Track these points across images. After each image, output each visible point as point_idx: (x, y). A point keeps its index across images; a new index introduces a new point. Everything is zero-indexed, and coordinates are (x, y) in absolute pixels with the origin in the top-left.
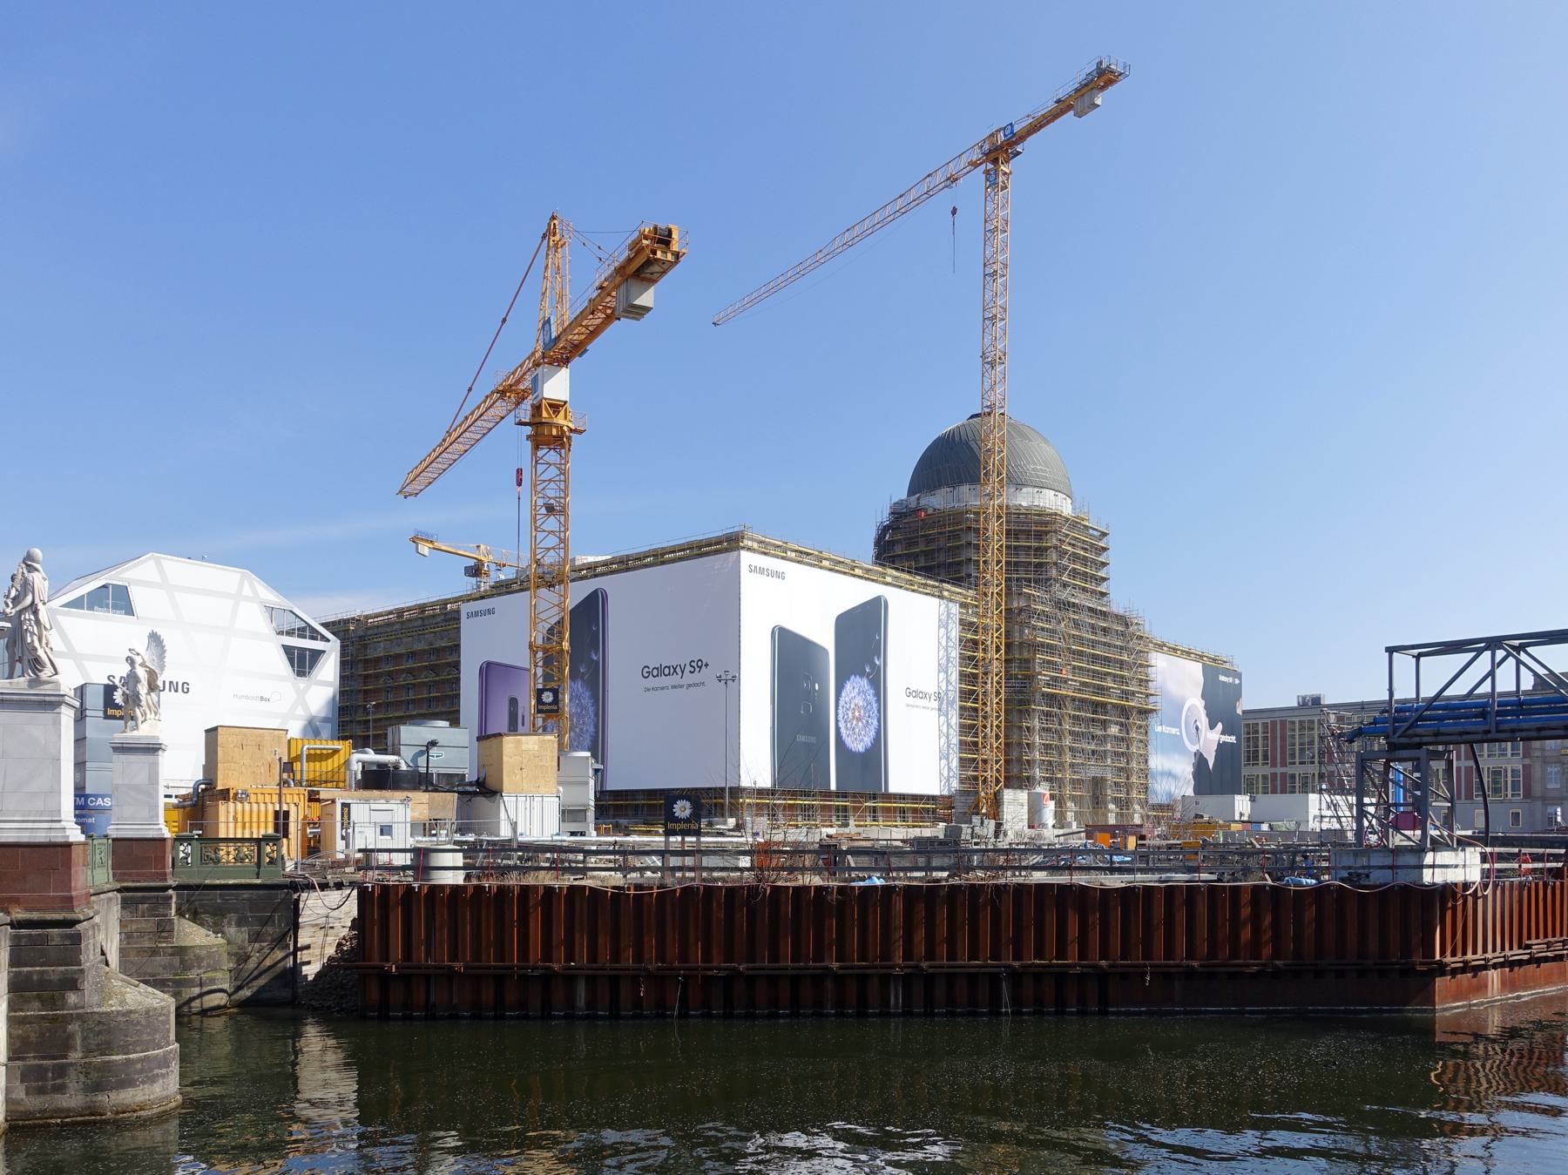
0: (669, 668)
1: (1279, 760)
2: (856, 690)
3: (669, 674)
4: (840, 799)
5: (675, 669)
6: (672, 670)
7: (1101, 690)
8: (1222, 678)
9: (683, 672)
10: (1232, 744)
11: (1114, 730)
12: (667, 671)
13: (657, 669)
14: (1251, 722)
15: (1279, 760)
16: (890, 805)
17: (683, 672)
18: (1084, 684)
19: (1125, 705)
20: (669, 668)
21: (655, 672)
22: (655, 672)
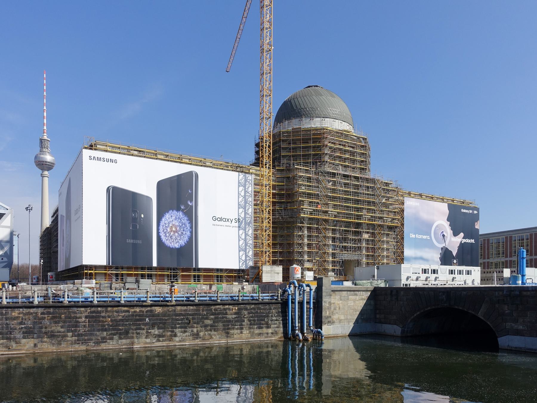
0: (225, 219)
1: (533, 253)
2: (173, 218)
3: (225, 221)
4: (150, 271)
5: (228, 220)
6: (227, 220)
7: (359, 217)
8: (463, 211)
9: (231, 222)
10: (472, 243)
11: (366, 236)
12: (224, 220)
13: (220, 218)
14: (520, 235)
15: (533, 253)
16: (132, 272)
17: (231, 222)
18: (338, 213)
19: (374, 224)
20: (225, 219)
21: (219, 219)
22: (219, 219)
